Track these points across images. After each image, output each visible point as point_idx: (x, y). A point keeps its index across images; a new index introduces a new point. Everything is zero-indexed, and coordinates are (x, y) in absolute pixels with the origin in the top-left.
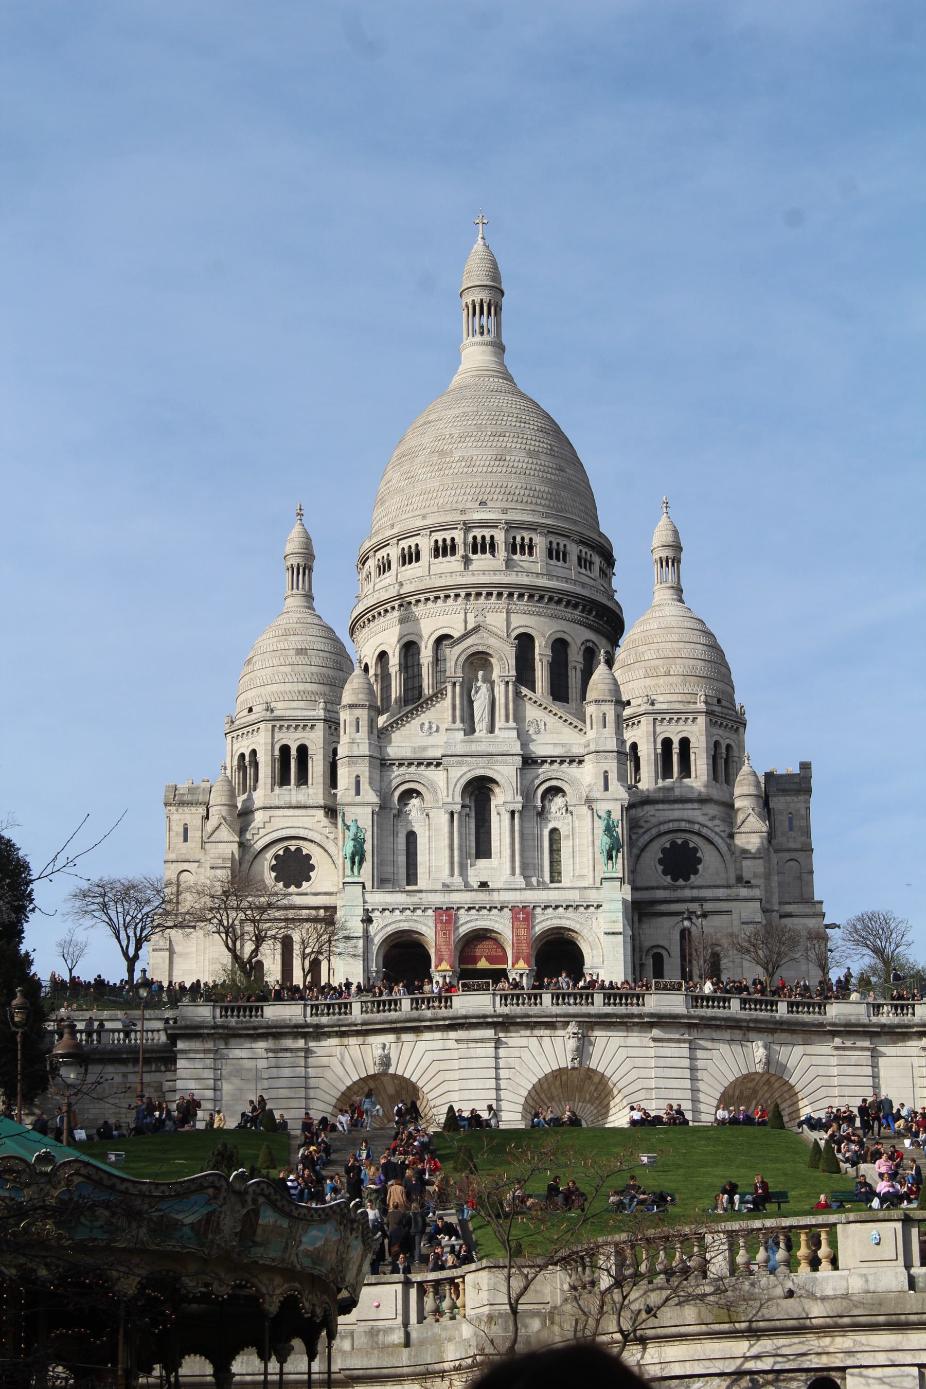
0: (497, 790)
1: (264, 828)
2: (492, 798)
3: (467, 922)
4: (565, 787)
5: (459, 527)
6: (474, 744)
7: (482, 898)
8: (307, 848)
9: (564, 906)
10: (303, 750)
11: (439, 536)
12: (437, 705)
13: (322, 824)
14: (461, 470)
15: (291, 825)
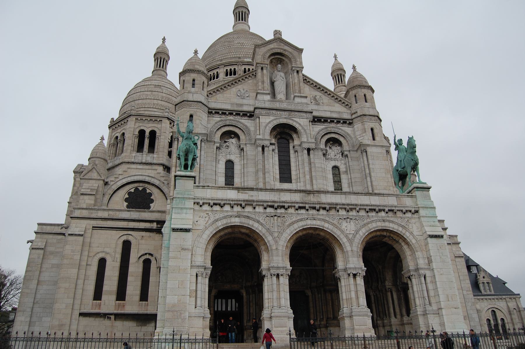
0: (294, 136)
1: (122, 175)
2: (291, 141)
3: (298, 221)
4: (341, 139)
5: (239, 63)
6: (278, 103)
7: (312, 199)
8: (150, 189)
9: (387, 209)
10: (153, 134)
11: (228, 68)
12: (249, 82)
13: (161, 175)
14: (238, 46)
15: (140, 174)
